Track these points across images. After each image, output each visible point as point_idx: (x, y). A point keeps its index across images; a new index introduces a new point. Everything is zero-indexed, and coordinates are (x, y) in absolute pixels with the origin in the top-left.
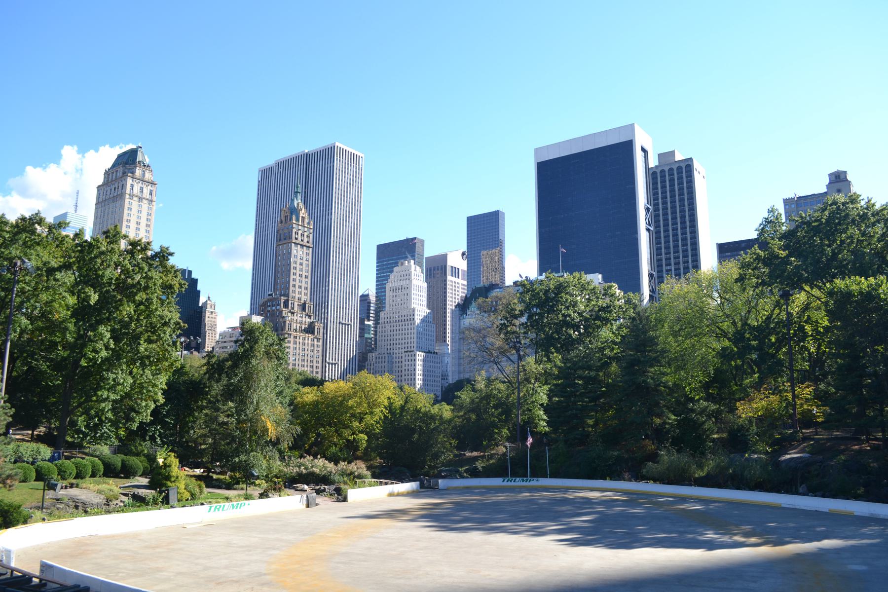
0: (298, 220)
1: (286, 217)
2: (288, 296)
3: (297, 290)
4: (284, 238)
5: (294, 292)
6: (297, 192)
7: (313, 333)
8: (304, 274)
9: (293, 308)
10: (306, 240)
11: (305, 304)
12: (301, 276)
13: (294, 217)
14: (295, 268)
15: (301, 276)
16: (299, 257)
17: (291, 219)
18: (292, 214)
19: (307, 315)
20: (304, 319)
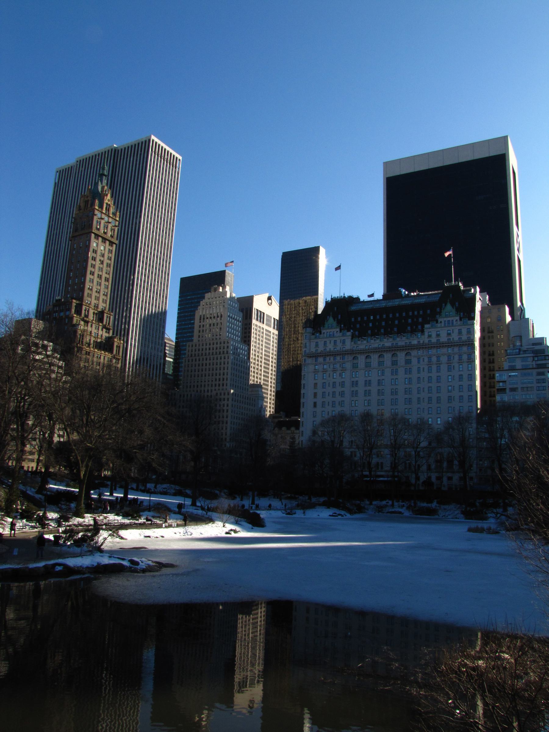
0: (101, 206)
1: (87, 202)
2: (81, 299)
3: (94, 294)
4: (82, 229)
5: (90, 296)
6: (103, 175)
7: (110, 350)
8: (104, 275)
9: (87, 316)
10: (109, 233)
11: (102, 313)
12: (100, 277)
13: (97, 201)
14: (93, 266)
15: (100, 277)
16: (99, 253)
17: (93, 204)
18: (94, 199)
19: (104, 327)
20: (100, 333)
